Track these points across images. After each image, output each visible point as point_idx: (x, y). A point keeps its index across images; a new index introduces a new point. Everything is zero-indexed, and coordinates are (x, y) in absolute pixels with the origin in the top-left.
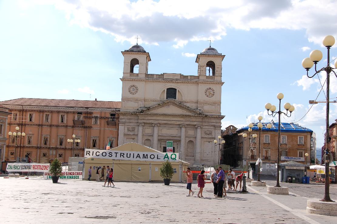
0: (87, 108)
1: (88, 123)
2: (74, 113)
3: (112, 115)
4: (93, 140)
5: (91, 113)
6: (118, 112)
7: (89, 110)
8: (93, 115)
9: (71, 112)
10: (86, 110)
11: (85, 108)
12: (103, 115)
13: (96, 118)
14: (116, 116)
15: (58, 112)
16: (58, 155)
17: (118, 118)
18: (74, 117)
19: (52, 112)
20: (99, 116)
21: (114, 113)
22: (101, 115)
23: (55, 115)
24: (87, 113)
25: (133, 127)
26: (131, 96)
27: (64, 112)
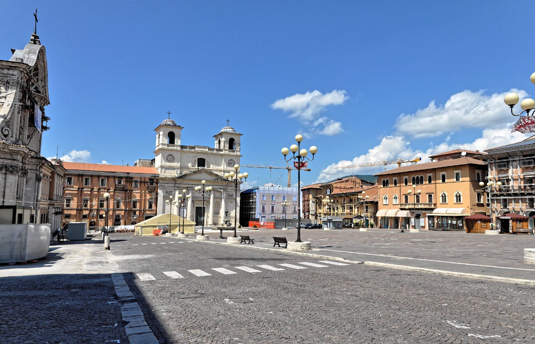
0: (128, 173)
1: (128, 187)
2: (115, 177)
3: (150, 179)
4: (134, 202)
5: (132, 178)
6: (158, 177)
7: (130, 175)
8: (133, 180)
9: (112, 177)
10: (127, 175)
11: (126, 173)
12: (143, 180)
13: (136, 182)
14: (155, 180)
15: (99, 176)
16: (99, 217)
17: (157, 183)
18: (115, 181)
19: (92, 176)
20: (139, 180)
21: (153, 178)
22: (141, 179)
23: (95, 180)
24: (126, 178)
25: (171, 190)
26: (168, 164)
27: (105, 176)
